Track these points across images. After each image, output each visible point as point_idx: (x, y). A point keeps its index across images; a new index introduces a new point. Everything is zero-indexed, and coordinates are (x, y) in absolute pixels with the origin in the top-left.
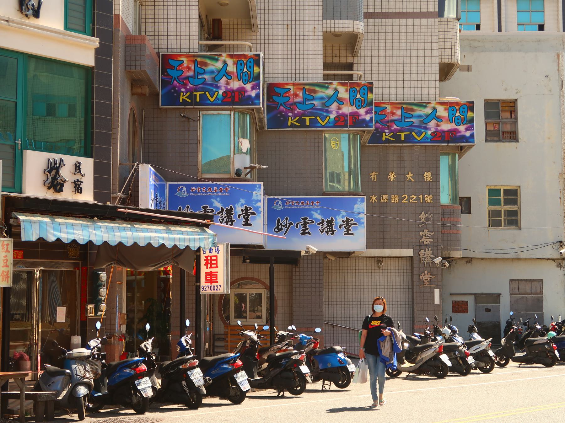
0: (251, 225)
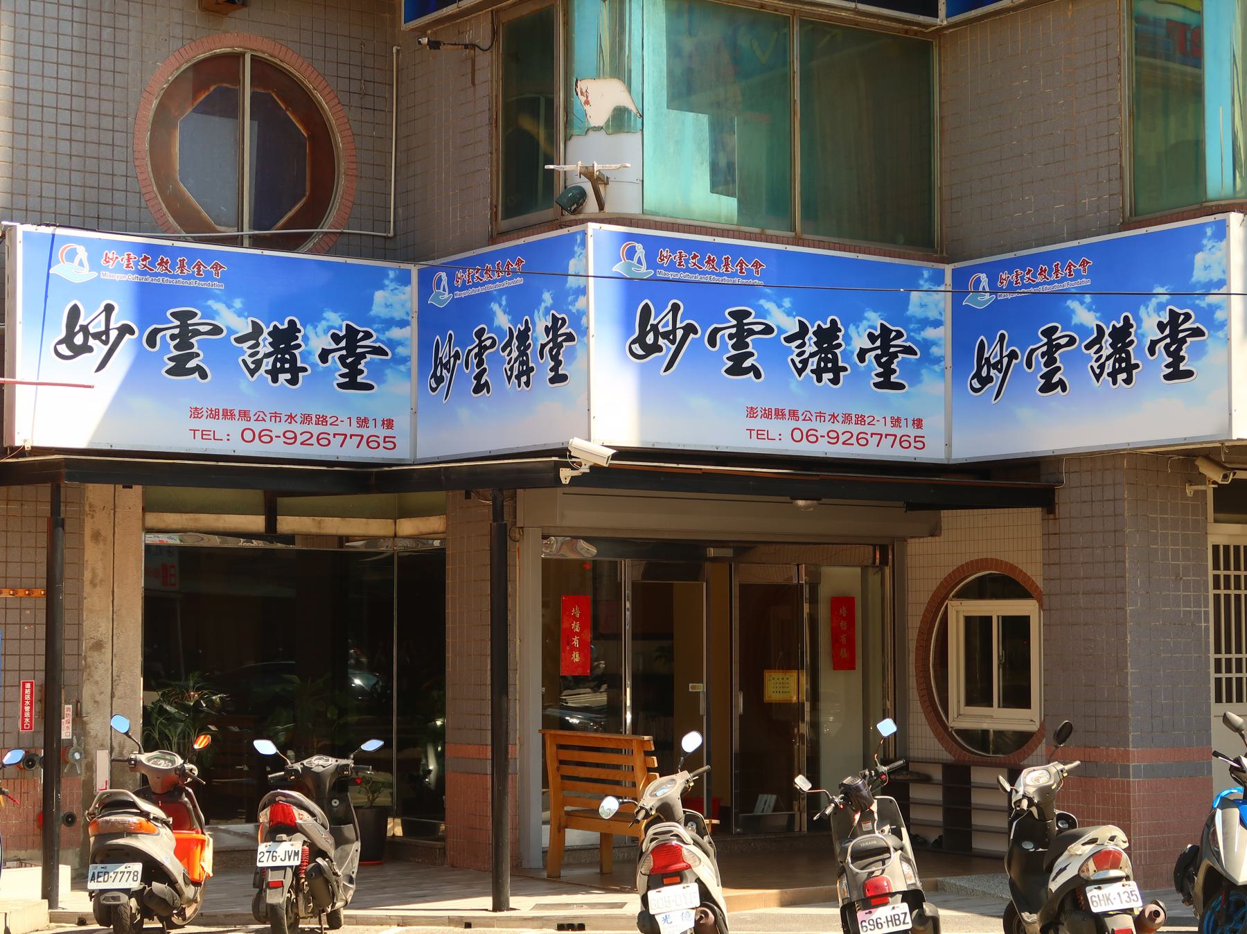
0: (1189, 374)
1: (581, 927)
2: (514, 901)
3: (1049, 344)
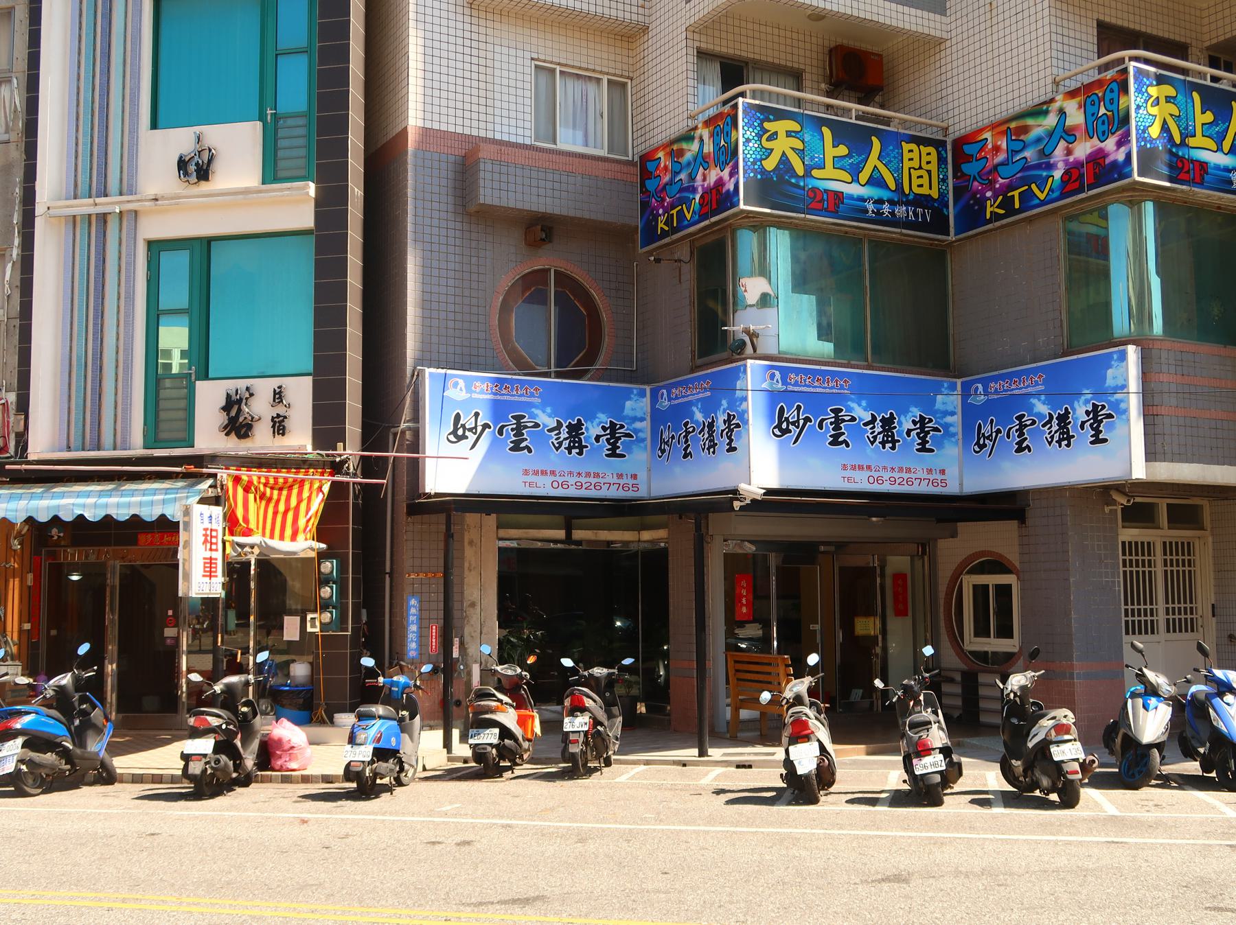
0: (1105, 440)
1: (750, 767)
2: (711, 751)
3: (1020, 424)
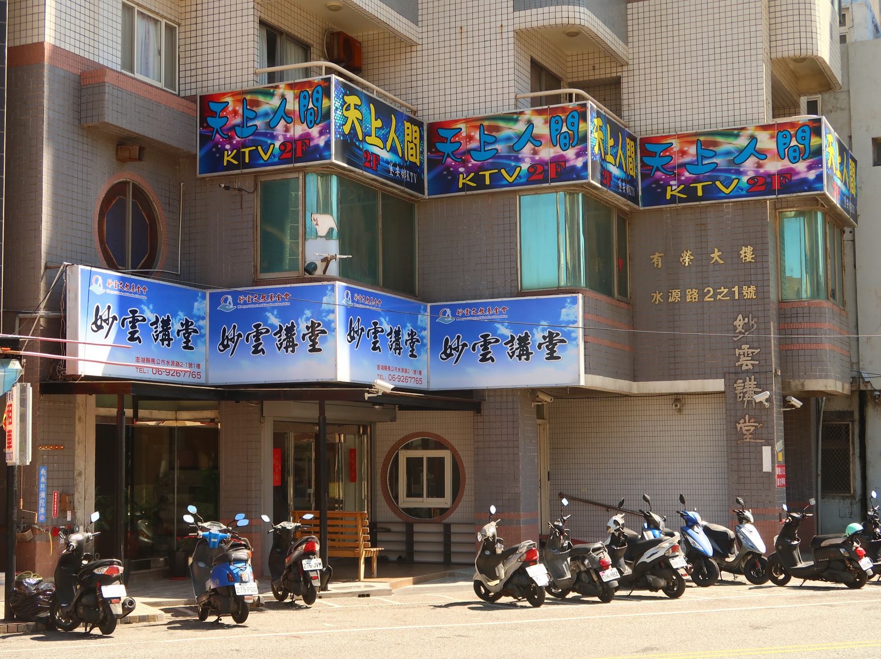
0: (320, 350)
1: (368, 595)
2: (330, 586)
3: (257, 331)
